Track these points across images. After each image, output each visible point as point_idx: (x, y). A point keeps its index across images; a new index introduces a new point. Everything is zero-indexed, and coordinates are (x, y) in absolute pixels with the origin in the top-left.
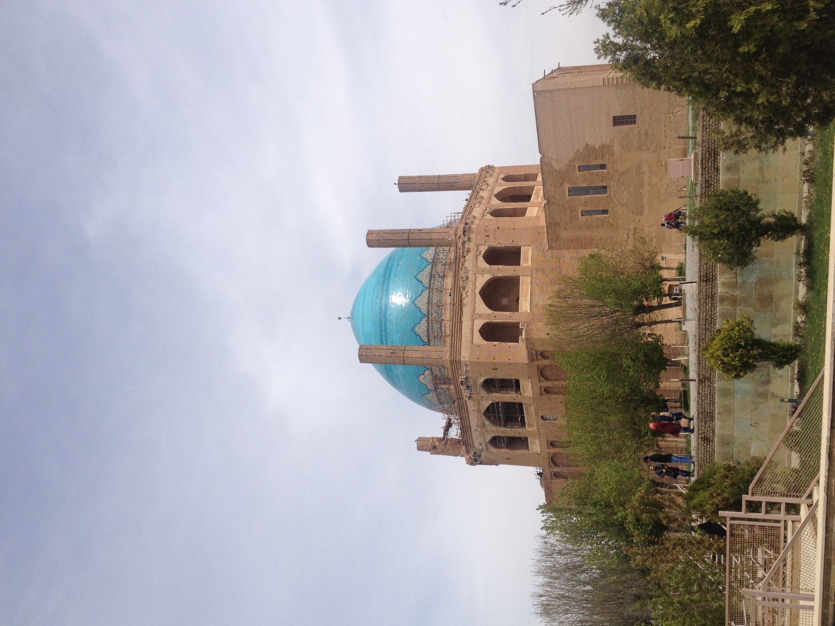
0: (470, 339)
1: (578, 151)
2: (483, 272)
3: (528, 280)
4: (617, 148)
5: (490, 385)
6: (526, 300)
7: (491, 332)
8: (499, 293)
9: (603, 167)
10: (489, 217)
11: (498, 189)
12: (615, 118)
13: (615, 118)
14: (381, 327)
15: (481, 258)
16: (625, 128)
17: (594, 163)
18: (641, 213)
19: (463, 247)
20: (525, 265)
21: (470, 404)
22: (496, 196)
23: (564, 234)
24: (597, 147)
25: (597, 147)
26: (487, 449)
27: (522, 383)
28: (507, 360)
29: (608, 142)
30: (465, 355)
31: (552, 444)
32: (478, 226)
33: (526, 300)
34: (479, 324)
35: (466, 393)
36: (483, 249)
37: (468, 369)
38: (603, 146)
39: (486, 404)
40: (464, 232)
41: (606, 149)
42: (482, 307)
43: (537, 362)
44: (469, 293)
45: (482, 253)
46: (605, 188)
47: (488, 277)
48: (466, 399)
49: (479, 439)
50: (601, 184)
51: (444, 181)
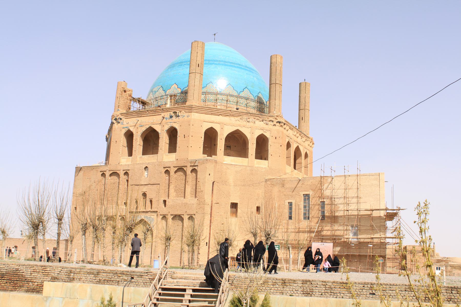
0: (207, 120)
3: (246, 164)
5: (173, 133)
7: (210, 136)
11: (301, 148)
14: (212, 61)
19: (270, 121)
20: (255, 162)
21: (159, 118)
23: (276, 190)
26: (123, 128)
27: (173, 155)
30: (195, 116)
31: (126, 174)
32: (282, 132)
34: (217, 127)
35: (167, 115)
36: (267, 135)
37: (186, 118)
39: (158, 128)
40: (280, 122)
43: (189, 165)
44: (238, 123)
45: (265, 134)
47: (248, 136)
48: (163, 114)
49: (130, 123)
51: (306, 113)
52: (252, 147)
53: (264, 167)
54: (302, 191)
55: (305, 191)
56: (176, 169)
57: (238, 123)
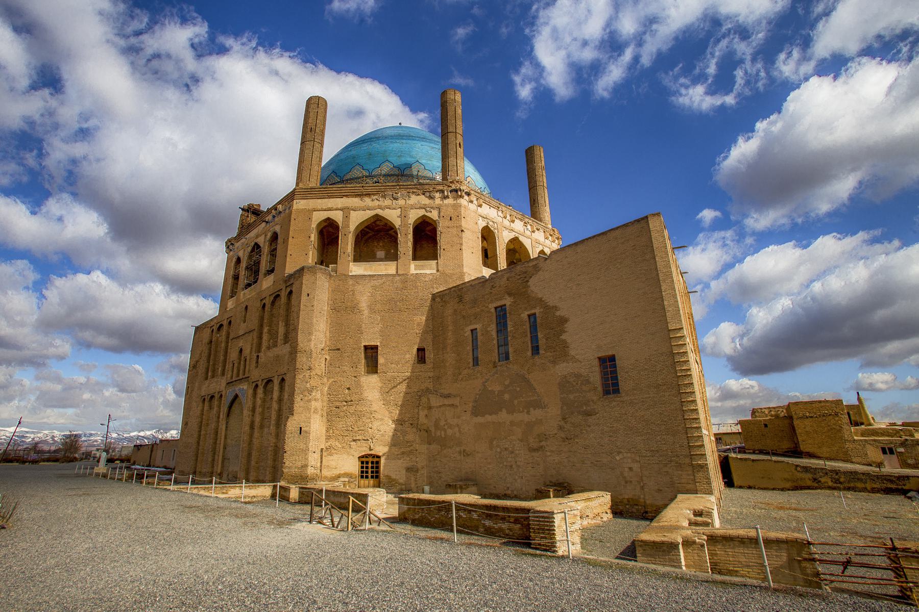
0: (319, 207)
1: (556, 308)
2: (403, 216)
4: (563, 369)
6: (365, 269)
8: (376, 237)
9: (536, 350)
10: (482, 224)
11: (527, 243)
12: (612, 359)
13: (612, 359)
15: (422, 212)
16: (596, 378)
17: (540, 335)
18: (476, 412)
20: (412, 266)
22: (515, 240)
24: (563, 337)
25: (563, 337)
28: (289, 252)
29: (572, 353)
33: (365, 269)
34: (338, 216)
36: (434, 215)
38: (565, 345)
39: (261, 241)
40: (456, 191)
41: (562, 352)
42: (357, 218)
44: (376, 203)
45: (428, 214)
46: (507, 358)
47: (397, 223)
50: (511, 350)
52: (406, 242)
53: (428, 272)
54: (492, 302)
55: (497, 300)
56: (272, 298)
57: (376, 203)
